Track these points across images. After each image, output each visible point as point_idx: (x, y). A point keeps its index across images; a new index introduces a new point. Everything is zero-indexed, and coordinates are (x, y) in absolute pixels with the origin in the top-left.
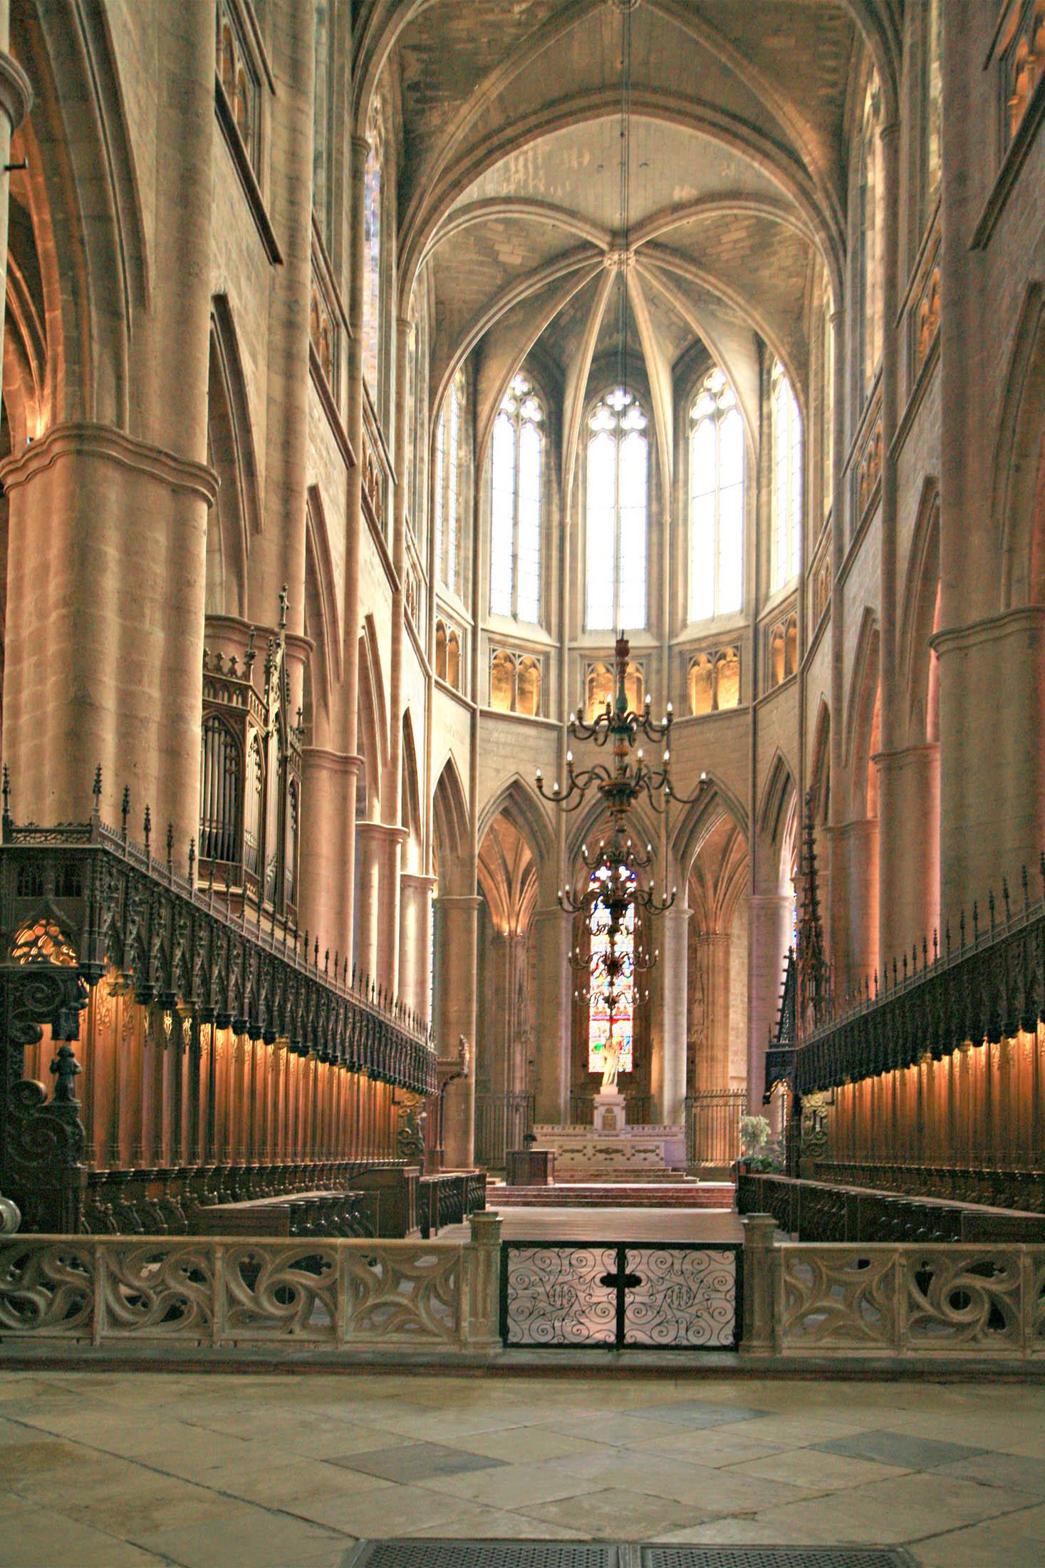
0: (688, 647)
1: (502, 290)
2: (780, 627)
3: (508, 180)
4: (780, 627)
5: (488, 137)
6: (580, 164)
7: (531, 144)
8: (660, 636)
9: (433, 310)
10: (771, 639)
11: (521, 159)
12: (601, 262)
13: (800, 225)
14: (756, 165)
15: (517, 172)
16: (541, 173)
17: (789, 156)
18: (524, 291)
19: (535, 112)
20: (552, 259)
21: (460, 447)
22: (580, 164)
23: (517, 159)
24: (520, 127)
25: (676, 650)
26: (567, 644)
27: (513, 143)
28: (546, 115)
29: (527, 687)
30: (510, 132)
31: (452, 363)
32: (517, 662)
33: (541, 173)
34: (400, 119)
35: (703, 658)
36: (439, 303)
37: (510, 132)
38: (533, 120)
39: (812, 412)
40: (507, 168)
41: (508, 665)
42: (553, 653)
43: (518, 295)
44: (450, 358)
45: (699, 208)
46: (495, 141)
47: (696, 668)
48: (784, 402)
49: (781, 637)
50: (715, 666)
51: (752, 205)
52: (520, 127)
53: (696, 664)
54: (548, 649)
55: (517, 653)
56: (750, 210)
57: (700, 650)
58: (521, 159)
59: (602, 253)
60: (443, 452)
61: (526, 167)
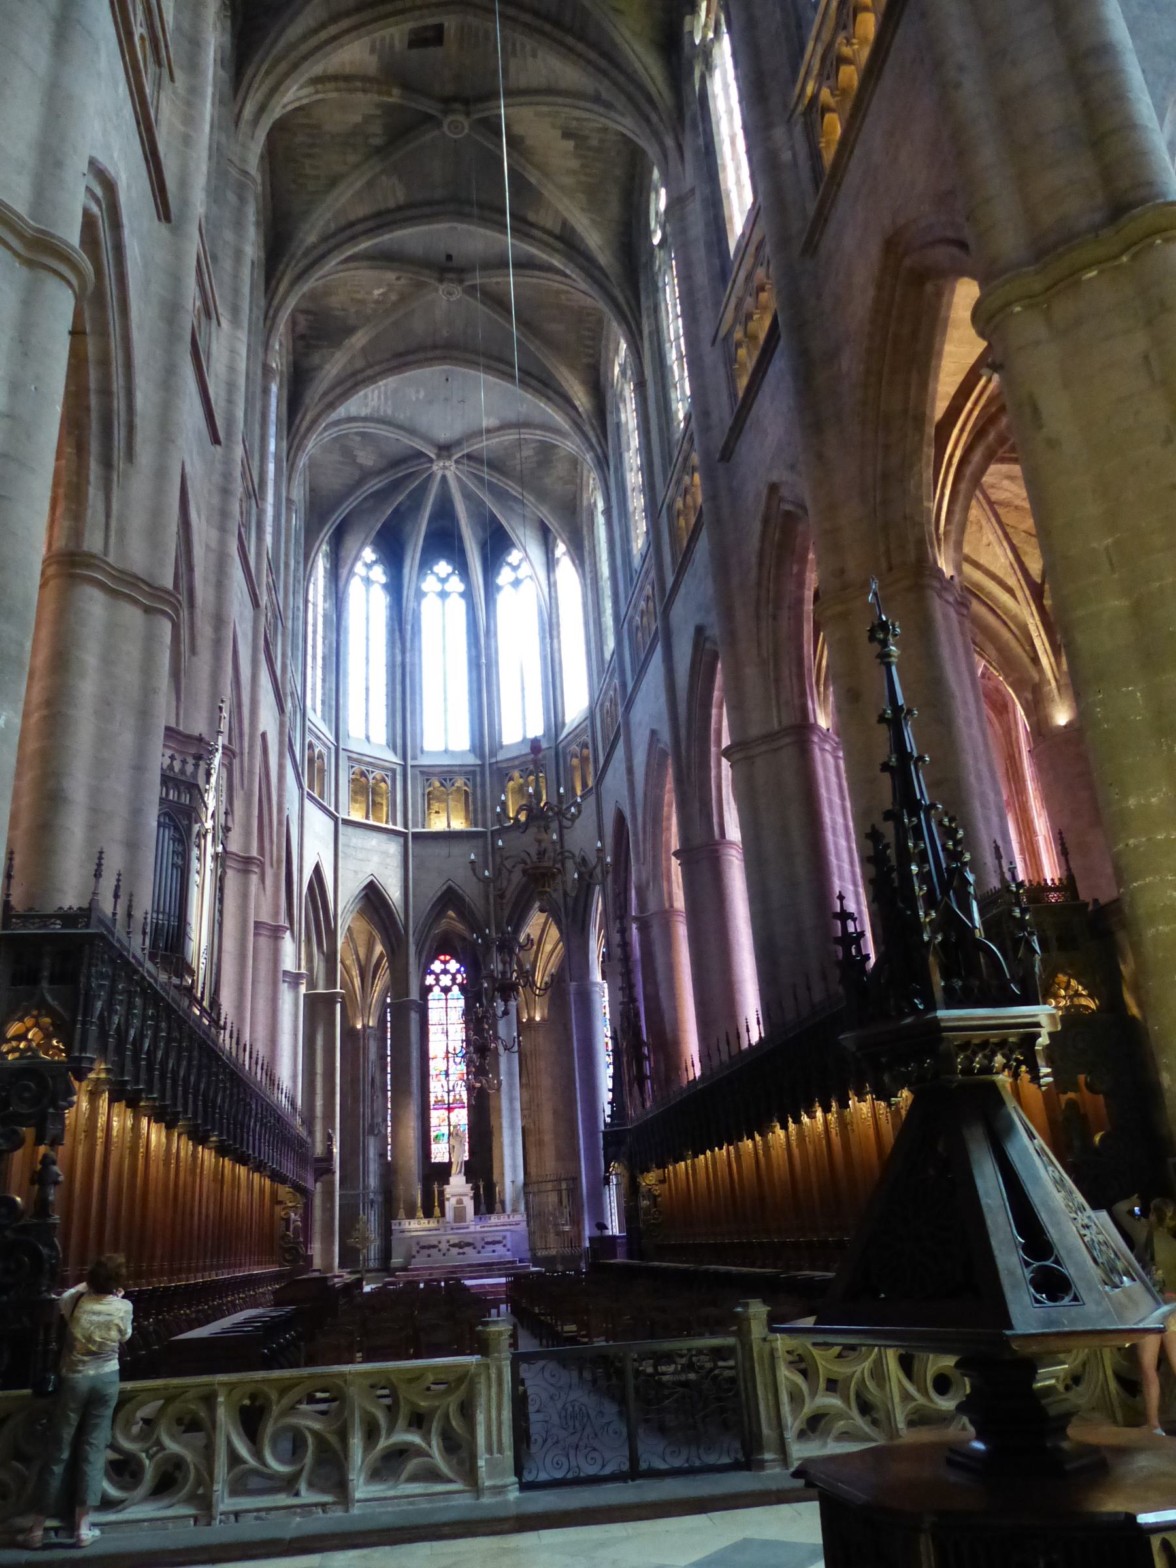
0: (504, 765)
1: (360, 483)
2: (574, 748)
3: (366, 406)
4: (574, 748)
5: (354, 374)
6: (417, 399)
7: (384, 381)
8: (482, 756)
9: (308, 496)
10: (569, 758)
11: (376, 392)
12: (431, 467)
13: (574, 447)
14: (542, 405)
15: (372, 400)
16: (390, 402)
17: (565, 401)
18: (375, 484)
19: (388, 360)
20: (396, 463)
21: (325, 601)
22: (417, 399)
23: (373, 391)
24: (377, 368)
25: (495, 767)
26: (410, 762)
27: (372, 380)
28: (394, 363)
29: (378, 800)
30: (370, 372)
31: (322, 535)
32: (370, 777)
33: (390, 402)
34: (291, 358)
35: (516, 774)
36: (312, 490)
37: (370, 372)
38: (385, 366)
39: (588, 581)
40: (366, 396)
41: (363, 779)
42: (399, 770)
43: (372, 487)
44: (320, 530)
45: (502, 432)
46: (359, 377)
47: (511, 783)
48: (566, 571)
49: (577, 757)
50: (526, 781)
51: (538, 432)
52: (377, 368)
53: (511, 779)
54: (394, 766)
55: (370, 769)
56: (539, 435)
57: (515, 767)
58: (376, 392)
59: (431, 461)
60: (313, 604)
61: (379, 398)
